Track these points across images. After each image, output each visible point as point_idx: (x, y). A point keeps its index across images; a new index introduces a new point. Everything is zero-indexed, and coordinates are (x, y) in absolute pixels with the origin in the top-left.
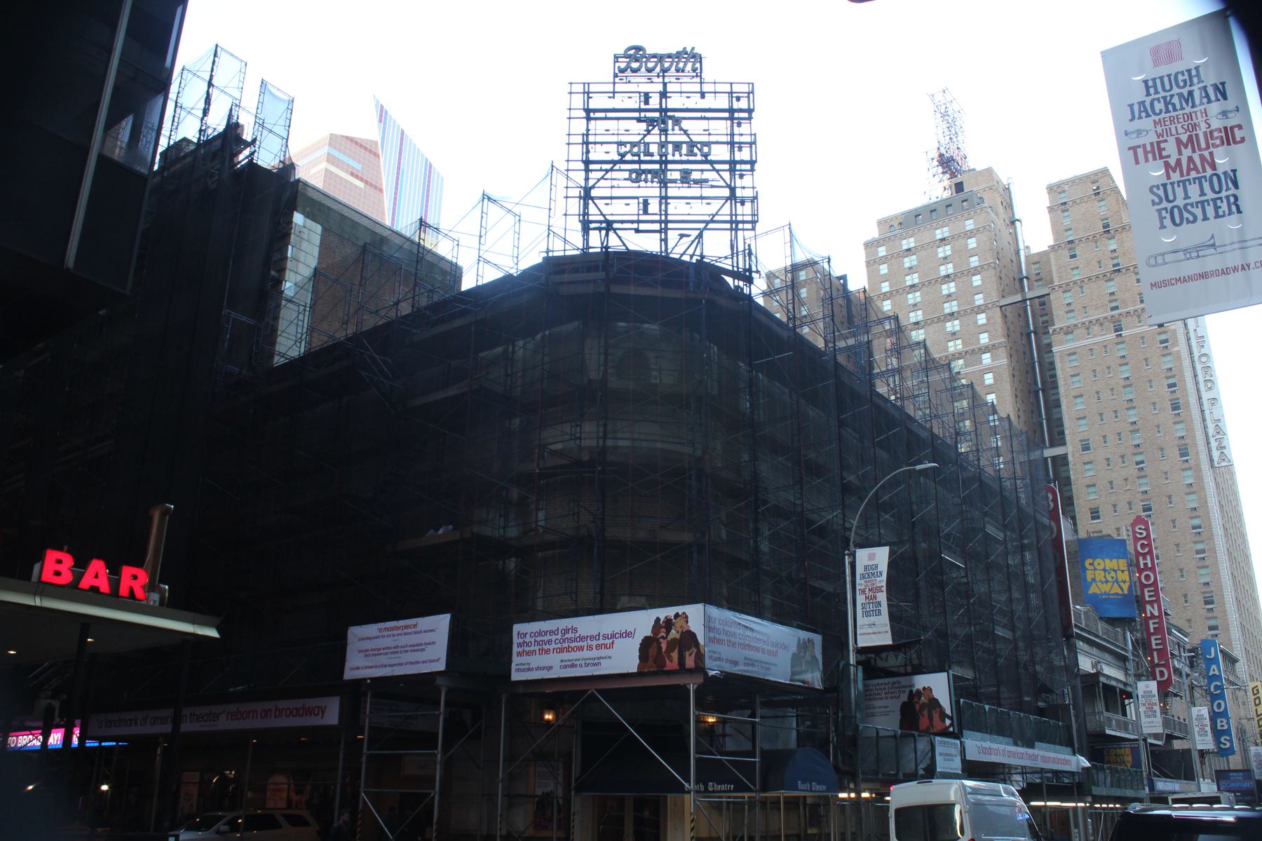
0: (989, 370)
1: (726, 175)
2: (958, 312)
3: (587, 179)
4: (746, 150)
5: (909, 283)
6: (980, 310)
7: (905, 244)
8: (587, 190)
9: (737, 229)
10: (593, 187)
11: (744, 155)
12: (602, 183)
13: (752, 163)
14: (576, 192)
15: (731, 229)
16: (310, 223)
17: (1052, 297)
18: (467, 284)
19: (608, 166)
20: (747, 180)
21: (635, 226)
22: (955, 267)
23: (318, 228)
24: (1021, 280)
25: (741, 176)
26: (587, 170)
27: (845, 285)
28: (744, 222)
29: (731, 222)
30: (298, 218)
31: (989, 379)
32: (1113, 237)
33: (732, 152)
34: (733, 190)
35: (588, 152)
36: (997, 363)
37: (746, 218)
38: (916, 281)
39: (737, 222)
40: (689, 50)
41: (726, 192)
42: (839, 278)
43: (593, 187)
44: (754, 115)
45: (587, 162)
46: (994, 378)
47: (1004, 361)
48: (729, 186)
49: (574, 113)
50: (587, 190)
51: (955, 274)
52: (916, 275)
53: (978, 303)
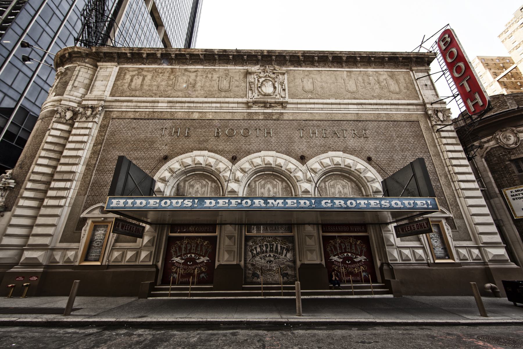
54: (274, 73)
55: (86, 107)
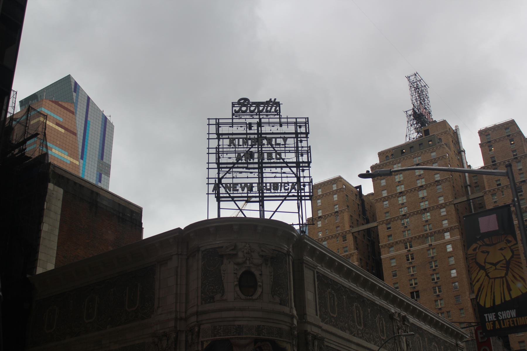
0: (449, 242)
1: (294, 170)
2: (429, 208)
3: (219, 173)
4: (305, 156)
5: (399, 191)
6: (442, 206)
7: (396, 168)
8: (220, 179)
9: (301, 200)
10: (223, 177)
11: (305, 158)
12: (228, 175)
13: (309, 163)
14: (212, 181)
15: (298, 200)
16: (56, 188)
17: (485, 198)
18: (151, 229)
19: (231, 166)
20: (306, 173)
21: (246, 199)
22: (426, 181)
23: (61, 191)
24: (466, 187)
25: (303, 171)
26: (219, 168)
27: (361, 191)
28: (305, 196)
29: (298, 196)
30: (51, 186)
31: (449, 248)
32: (519, 161)
33: (297, 157)
34: (299, 178)
35: (219, 158)
36: (454, 238)
37: (306, 194)
38: (403, 190)
39: (302, 196)
40: (273, 100)
41: (295, 180)
42: (357, 188)
43: (223, 177)
44: (311, 165)
45: (218, 163)
46: (453, 247)
47: (458, 237)
48: (296, 176)
49: (211, 136)
50: (220, 179)
51: (426, 185)
52: (403, 186)
53: (441, 202)
54: (404, 324)
55: (315, 337)
